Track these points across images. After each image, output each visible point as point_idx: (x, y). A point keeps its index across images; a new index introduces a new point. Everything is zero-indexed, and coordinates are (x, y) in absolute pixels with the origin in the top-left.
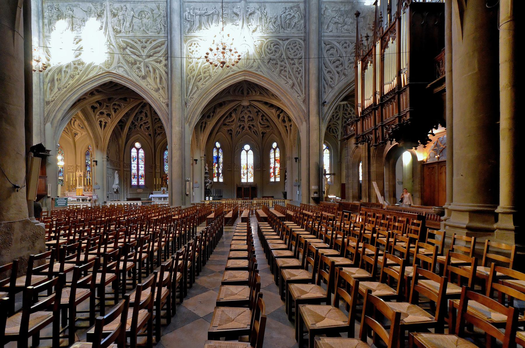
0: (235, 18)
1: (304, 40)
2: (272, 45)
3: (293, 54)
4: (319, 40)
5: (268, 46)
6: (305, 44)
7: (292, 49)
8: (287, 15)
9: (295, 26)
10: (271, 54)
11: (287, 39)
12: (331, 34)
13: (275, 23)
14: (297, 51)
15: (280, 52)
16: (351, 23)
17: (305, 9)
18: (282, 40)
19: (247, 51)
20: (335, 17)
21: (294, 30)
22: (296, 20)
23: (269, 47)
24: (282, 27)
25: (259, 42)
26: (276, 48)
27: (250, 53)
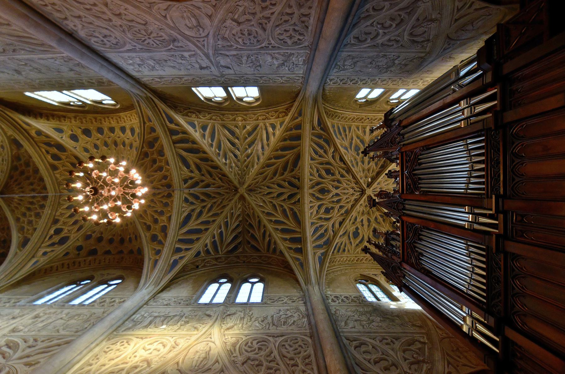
0: (206, 318)
1: (311, 337)
2: (255, 342)
3: (292, 353)
4: (334, 330)
5: (247, 343)
6: (314, 341)
7: (291, 346)
8: (281, 315)
9: (293, 323)
10: (251, 351)
11: (282, 336)
12: (353, 330)
13: (262, 321)
14: (300, 348)
15: (267, 350)
16: (380, 320)
17: (307, 310)
18: (273, 337)
19: (208, 349)
20: (353, 316)
21: (293, 327)
22: (295, 319)
23: (250, 344)
24: (274, 325)
25: (234, 339)
26: (262, 345)
27: (212, 352)
